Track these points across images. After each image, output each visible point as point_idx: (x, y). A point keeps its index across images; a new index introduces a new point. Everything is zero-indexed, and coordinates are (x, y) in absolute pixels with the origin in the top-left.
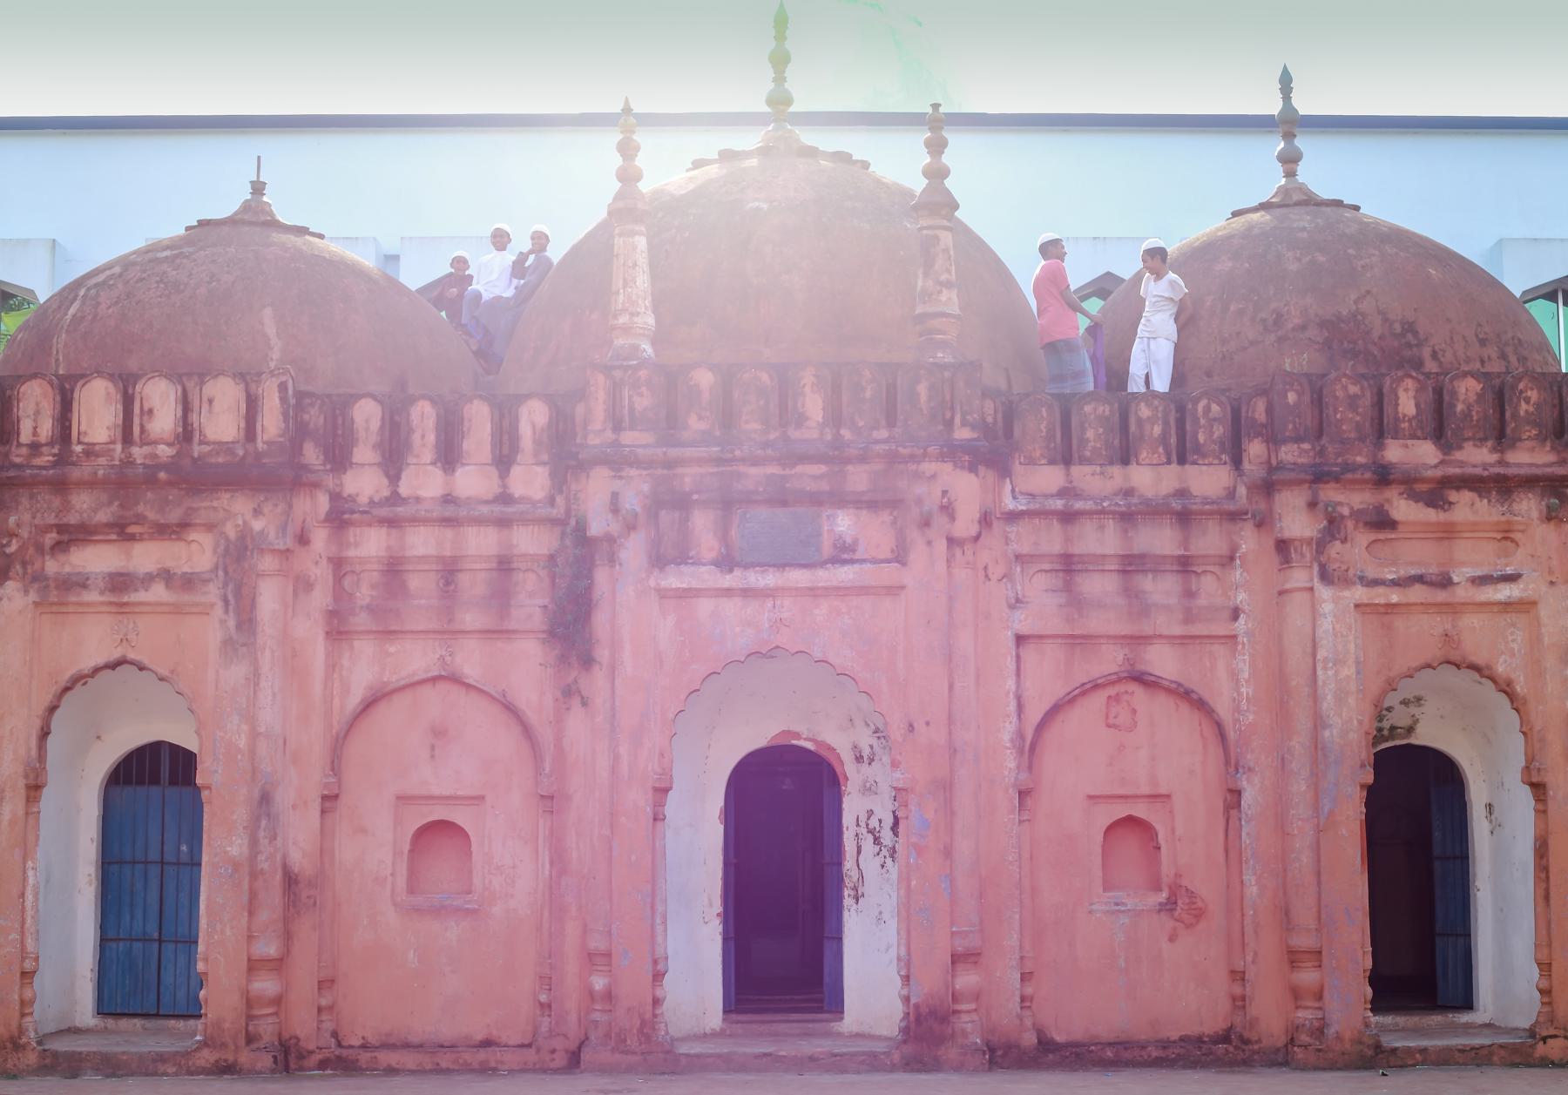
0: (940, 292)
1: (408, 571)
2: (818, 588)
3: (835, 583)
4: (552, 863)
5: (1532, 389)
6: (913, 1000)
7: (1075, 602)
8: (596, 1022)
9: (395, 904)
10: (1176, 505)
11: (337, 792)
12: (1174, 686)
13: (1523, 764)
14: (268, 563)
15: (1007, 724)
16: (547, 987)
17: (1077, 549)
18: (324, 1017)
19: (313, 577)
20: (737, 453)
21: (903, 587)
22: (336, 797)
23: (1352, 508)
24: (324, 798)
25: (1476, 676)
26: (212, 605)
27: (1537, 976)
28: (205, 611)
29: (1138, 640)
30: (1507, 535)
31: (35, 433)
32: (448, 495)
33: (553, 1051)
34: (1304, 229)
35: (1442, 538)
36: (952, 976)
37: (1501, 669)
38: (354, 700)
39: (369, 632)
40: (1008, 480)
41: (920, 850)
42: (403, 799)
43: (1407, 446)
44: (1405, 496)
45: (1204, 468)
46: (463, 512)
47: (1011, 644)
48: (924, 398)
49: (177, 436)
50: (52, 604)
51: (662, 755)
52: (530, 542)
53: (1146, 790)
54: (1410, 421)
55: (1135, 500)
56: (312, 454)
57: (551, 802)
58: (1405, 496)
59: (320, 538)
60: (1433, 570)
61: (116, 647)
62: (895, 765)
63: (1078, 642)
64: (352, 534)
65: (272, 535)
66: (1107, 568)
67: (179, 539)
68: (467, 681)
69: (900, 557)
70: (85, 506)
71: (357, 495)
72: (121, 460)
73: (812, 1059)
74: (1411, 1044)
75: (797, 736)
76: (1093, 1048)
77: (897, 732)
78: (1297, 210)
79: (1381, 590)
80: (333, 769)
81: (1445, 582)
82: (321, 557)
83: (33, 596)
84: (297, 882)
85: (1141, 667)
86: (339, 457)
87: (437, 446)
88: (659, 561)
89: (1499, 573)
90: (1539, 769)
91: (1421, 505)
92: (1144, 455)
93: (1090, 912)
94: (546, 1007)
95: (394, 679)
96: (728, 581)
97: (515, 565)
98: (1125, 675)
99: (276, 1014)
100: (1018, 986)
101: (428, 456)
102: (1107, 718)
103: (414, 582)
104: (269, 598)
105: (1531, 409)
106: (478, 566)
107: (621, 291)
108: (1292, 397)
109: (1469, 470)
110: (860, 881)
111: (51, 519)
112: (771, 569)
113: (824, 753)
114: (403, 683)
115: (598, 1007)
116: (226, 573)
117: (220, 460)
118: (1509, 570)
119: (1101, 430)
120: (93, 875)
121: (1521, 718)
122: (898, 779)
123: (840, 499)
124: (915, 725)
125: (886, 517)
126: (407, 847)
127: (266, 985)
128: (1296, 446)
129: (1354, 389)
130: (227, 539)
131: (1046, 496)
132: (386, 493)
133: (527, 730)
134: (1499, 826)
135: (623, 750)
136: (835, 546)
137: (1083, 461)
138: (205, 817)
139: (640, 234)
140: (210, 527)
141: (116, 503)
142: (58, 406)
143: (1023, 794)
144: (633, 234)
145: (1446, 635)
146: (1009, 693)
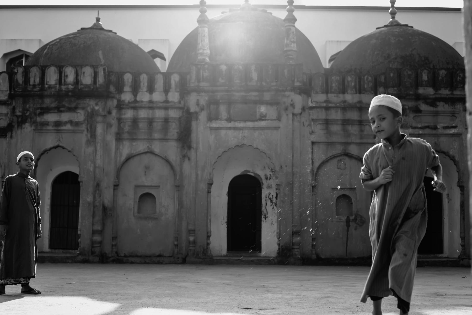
0: (291, 44)
1: (139, 122)
2: (255, 127)
3: (260, 126)
4: (179, 205)
5: (461, 73)
6: (281, 245)
7: (329, 133)
8: (190, 250)
9: (134, 216)
10: (358, 105)
11: (118, 184)
12: (357, 157)
13: (457, 180)
14: (99, 119)
15: (309, 167)
16: (177, 240)
17: (330, 118)
18: (114, 248)
19: (112, 123)
20: (233, 89)
21: (279, 127)
22: (118, 185)
23: (409, 107)
24: (115, 186)
25: (444, 156)
26: (84, 131)
27: (461, 242)
28: (82, 132)
29: (347, 144)
30: (453, 115)
31: (34, 82)
32: (151, 100)
33: (178, 258)
34: (396, 32)
35: (435, 116)
36: (292, 239)
37: (451, 153)
38: (123, 158)
39: (128, 139)
40: (310, 98)
41: (283, 202)
42: (137, 187)
43: (425, 89)
44: (424, 103)
45: (366, 95)
46: (155, 105)
47: (310, 144)
48: (286, 74)
49: (74, 83)
50: (39, 130)
51: (210, 174)
52: (173, 114)
53: (348, 187)
54: (426, 82)
55: (346, 104)
56: (112, 89)
57: (178, 187)
58: (424, 103)
59: (114, 112)
60: (432, 124)
61: (56, 142)
62: (277, 178)
63: (330, 144)
64: (123, 111)
65: (101, 110)
66: (338, 123)
67: (75, 112)
68: (155, 153)
69: (279, 119)
70: (48, 102)
71: (125, 100)
72: (58, 89)
73: (252, 261)
74: (424, 260)
75: (249, 172)
76: (332, 260)
77: (277, 169)
78: (395, 27)
79: (417, 130)
80: (117, 177)
81: (435, 128)
82: (114, 118)
83: (33, 128)
84: (106, 209)
85: (347, 151)
86: (120, 90)
87: (148, 86)
88: (210, 119)
89: (451, 126)
90: (462, 182)
91: (428, 106)
92: (349, 91)
93: (332, 221)
94: (176, 246)
95: (135, 152)
96: (230, 125)
97: (169, 120)
98: (343, 154)
99: (100, 246)
100: (311, 241)
101: (145, 89)
102: (338, 166)
103: (141, 125)
104: (99, 129)
105: (461, 79)
106: (159, 121)
107: (200, 43)
108: (392, 75)
109: (443, 96)
110: (267, 214)
111: (39, 106)
112: (242, 122)
113: (257, 177)
114: (137, 153)
115: (191, 245)
116: (88, 121)
117: (87, 89)
118: (454, 125)
119: (337, 84)
120: (49, 209)
121: (457, 167)
122: (277, 182)
123: (261, 102)
124: (283, 166)
125: (275, 107)
126: (138, 200)
127: (97, 238)
128: (393, 89)
129: (410, 73)
130: (88, 112)
131: (321, 102)
132: (133, 100)
133: (172, 167)
134: (451, 200)
135: (199, 173)
136: (260, 115)
137: (332, 92)
138: (81, 190)
139: (206, 27)
140: (83, 109)
141: (57, 102)
142: (41, 74)
143: (313, 187)
144: (204, 27)
145: (436, 143)
146: (309, 158)
